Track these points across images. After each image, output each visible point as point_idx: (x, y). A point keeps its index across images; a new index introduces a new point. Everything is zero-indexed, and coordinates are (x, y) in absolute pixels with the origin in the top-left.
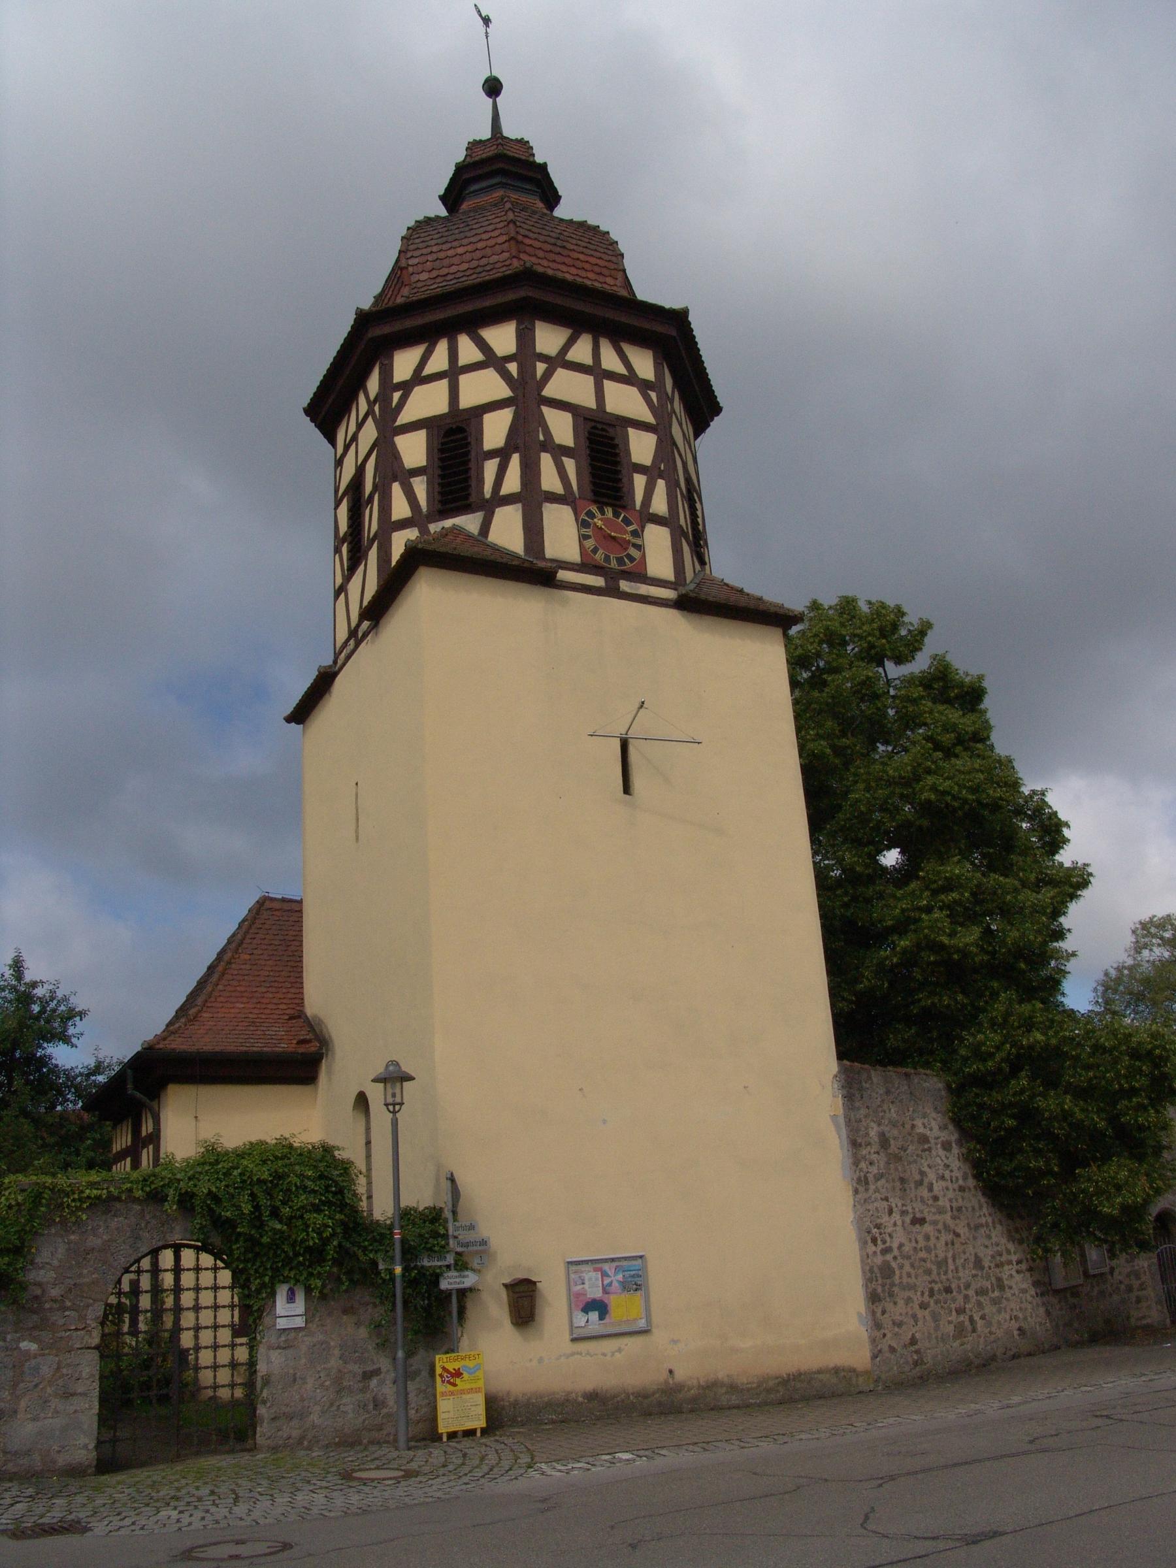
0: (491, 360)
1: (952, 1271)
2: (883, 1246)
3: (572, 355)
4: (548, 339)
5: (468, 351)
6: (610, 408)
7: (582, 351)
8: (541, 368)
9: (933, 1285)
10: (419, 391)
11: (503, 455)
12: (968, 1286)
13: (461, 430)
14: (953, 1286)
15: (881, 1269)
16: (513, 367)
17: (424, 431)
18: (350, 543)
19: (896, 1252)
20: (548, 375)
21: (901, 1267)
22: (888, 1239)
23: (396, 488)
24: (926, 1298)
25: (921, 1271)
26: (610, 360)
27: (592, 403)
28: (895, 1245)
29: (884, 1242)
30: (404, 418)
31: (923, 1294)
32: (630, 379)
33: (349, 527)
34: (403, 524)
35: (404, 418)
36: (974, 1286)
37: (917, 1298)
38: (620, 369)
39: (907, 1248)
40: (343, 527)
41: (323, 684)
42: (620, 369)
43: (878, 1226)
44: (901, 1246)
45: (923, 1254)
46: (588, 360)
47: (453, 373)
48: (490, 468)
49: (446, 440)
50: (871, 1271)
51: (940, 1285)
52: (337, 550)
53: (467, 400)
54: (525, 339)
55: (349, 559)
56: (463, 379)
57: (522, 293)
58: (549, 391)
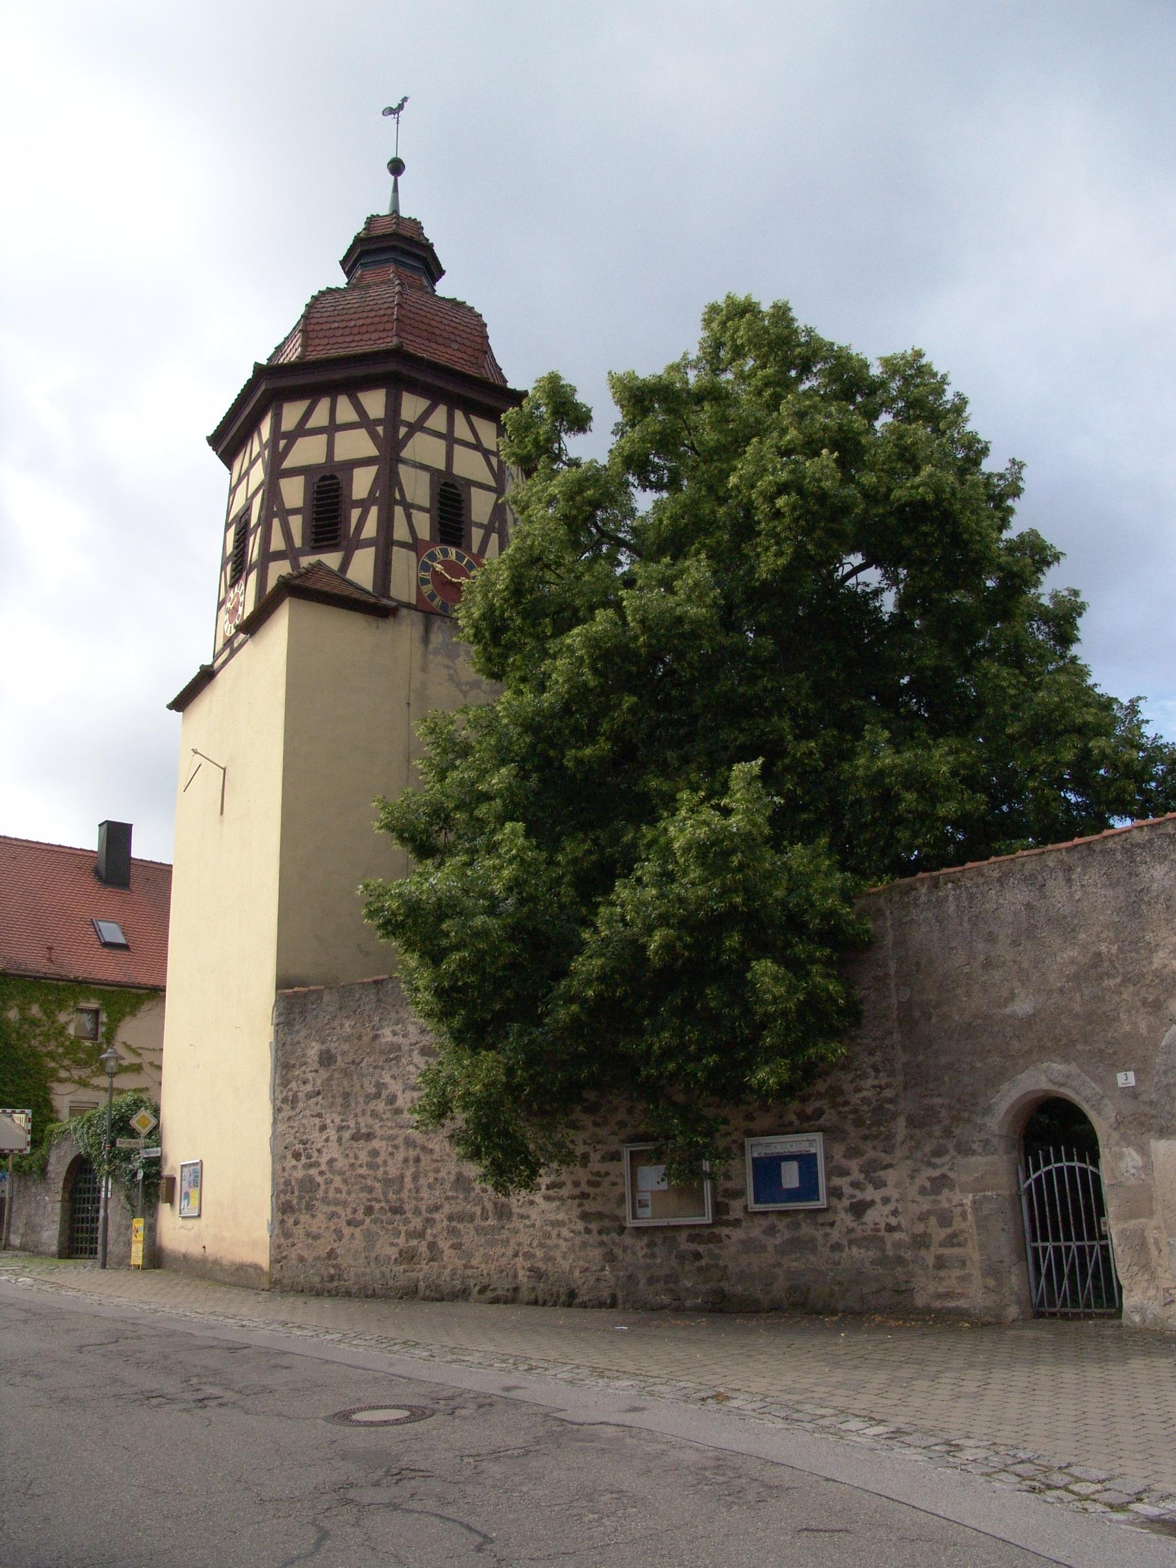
0: (365, 422)
1: (410, 1191)
2: (308, 1161)
3: (430, 423)
4: (412, 406)
5: (345, 411)
6: (457, 470)
7: (438, 419)
8: (403, 431)
9: (373, 1203)
10: (301, 443)
11: (364, 505)
12: (437, 1208)
13: (333, 477)
14: (406, 1207)
15: (301, 1183)
16: (380, 429)
17: (303, 477)
18: (234, 563)
19: (324, 1167)
20: (409, 436)
21: (329, 1182)
22: (315, 1154)
23: (276, 522)
24: (360, 1215)
25: (356, 1187)
26: (462, 430)
27: (442, 467)
28: (324, 1160)
29: (309, 1157)
30: (287, 464)
31: (355, 1211)
32: (477, 446)
33: (235, 548)
34: (279, 556)
35: (287, 464)
36: (447, 1209)
37: (345, 1214)
38: (470, 438)
39: (341, 1164)
40: (230, 549)
41: (206, 676)
42: (470, 438)
43: (304, 1143)
44: (331, 1162)
45: (363, 1171)
46: (443, 429)
47: (332, 428)
48: (355, 513)
49: (322, 484)
50: (287, 1183)
51: (383, 1204)
52: (223, 568)
53: (340, 455)
54: (393, 408)
55: (232, 577)
56: (339, 436)
57: (392, 366)
58: (406, 453)
